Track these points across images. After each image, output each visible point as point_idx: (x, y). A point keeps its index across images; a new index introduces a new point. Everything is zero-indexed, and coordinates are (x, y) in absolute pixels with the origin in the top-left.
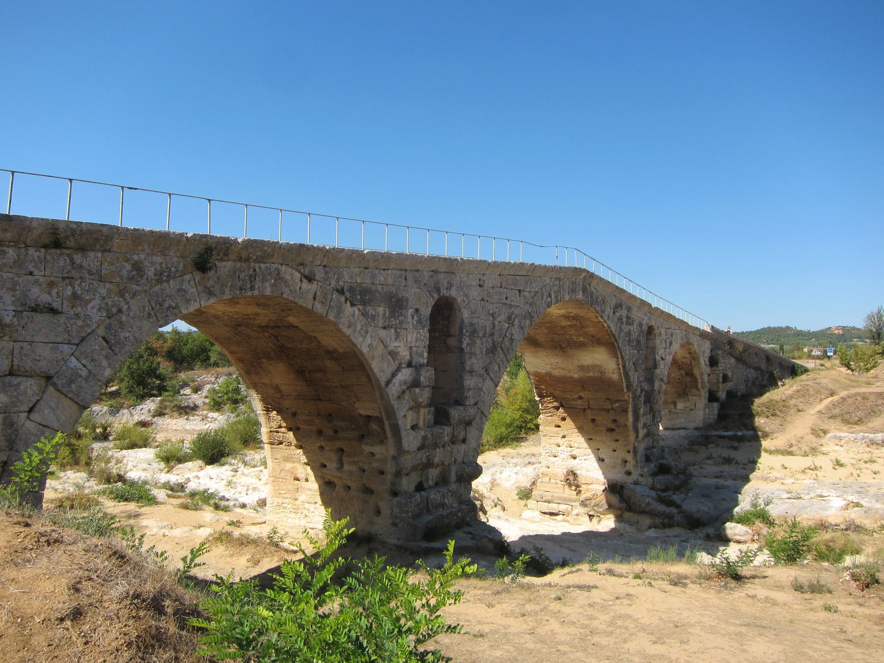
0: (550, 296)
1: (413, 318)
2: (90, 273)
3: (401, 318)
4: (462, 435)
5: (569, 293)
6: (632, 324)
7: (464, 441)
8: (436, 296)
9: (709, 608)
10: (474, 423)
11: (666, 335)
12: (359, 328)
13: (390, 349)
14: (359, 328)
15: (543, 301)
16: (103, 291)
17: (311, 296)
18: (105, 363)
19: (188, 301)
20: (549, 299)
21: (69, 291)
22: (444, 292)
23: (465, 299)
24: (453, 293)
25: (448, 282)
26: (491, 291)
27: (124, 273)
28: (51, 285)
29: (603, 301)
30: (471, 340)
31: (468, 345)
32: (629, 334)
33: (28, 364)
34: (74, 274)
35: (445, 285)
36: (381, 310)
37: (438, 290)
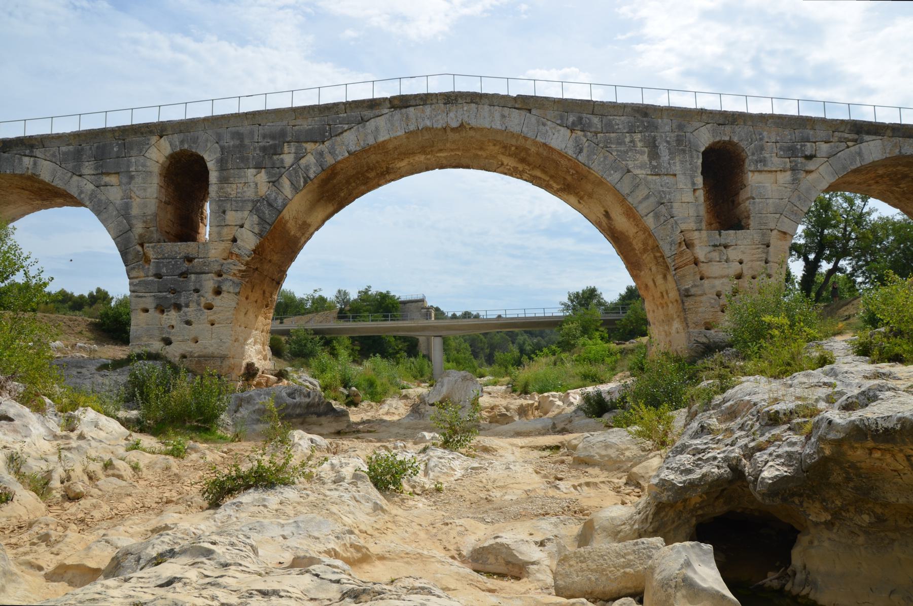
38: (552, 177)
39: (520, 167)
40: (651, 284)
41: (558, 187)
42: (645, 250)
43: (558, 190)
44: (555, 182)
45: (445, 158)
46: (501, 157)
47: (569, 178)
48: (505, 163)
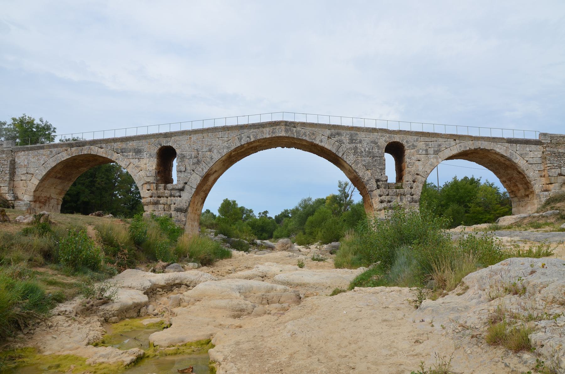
0: (249, 137)
1: (147, 154)
2: (41, 154)
3: (140, 155)
4: (178, 194)
5: (269, 134)
6: (360, 142)
7: (180, 197)
8: (159, 147)
9: (238, 269)
10: (185, 190)
11: (427, 145)
12: (121, 159)
13: (135, 165)
14: (121, 159)
15: (242, 140)
16: (44, 157)
17: (102, 152)
18: (44, 171)
19: (63, 157)
20: (249, 139)
21: (37, 158)
22: (165, 145)
23: (177, 145)
24: (170, 144)
25: (166, 141)
26: (196, 141)
27: (48, 153)
28: (34, 157)
29: (313, 134)
30: (182, 160)
31: (180, 162)
32: (356, 148)
33: (29, 172)
34: (38, 155)
35: (164, 142)
36: (131, 154)
37: (161, 145)
38: (238, 153)
39: (251, 146)
40: (196, 203)
41: (232, 154)
42: (204, 191)
43: (231, 153)
44: (235, 154)
45: (285, 139)
46: (261, 143)
47: (233, 158)
48: (257, 143)
